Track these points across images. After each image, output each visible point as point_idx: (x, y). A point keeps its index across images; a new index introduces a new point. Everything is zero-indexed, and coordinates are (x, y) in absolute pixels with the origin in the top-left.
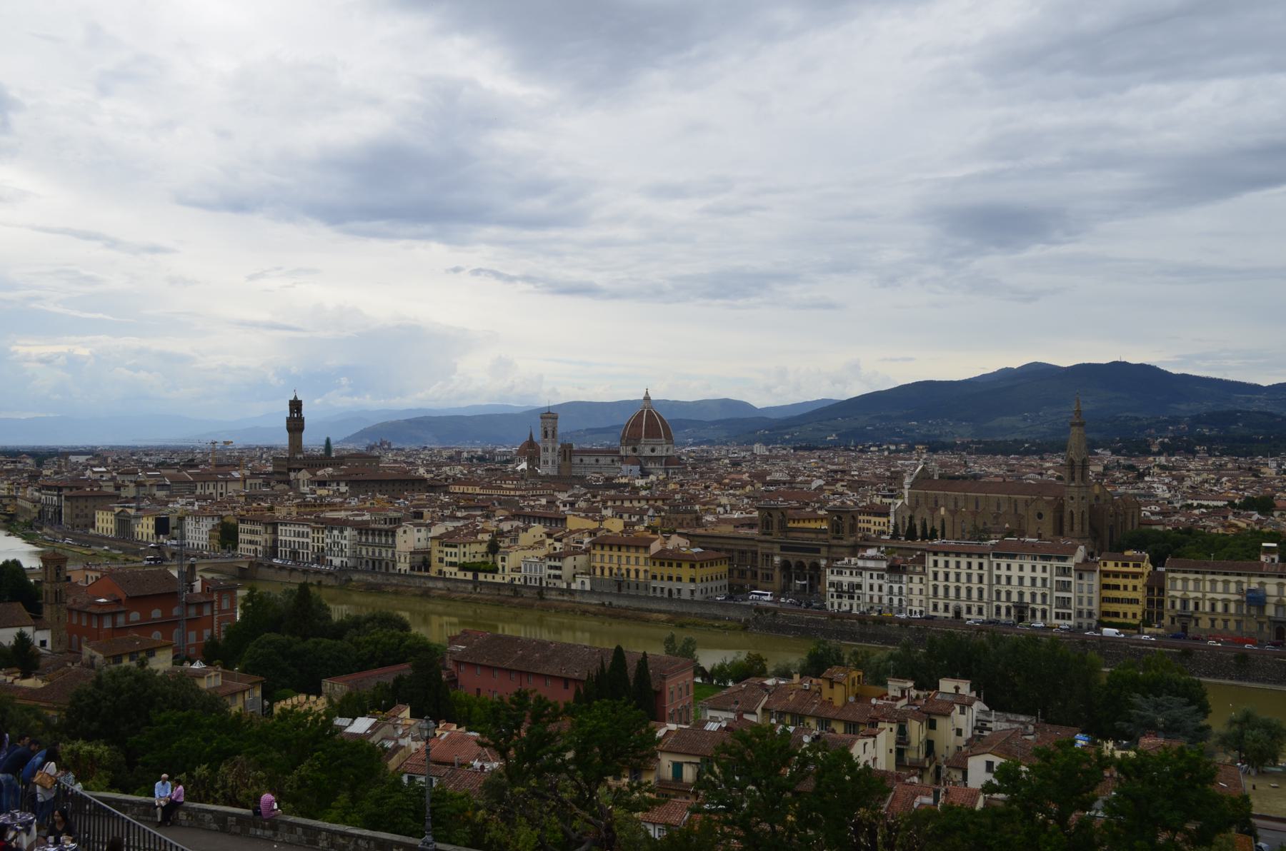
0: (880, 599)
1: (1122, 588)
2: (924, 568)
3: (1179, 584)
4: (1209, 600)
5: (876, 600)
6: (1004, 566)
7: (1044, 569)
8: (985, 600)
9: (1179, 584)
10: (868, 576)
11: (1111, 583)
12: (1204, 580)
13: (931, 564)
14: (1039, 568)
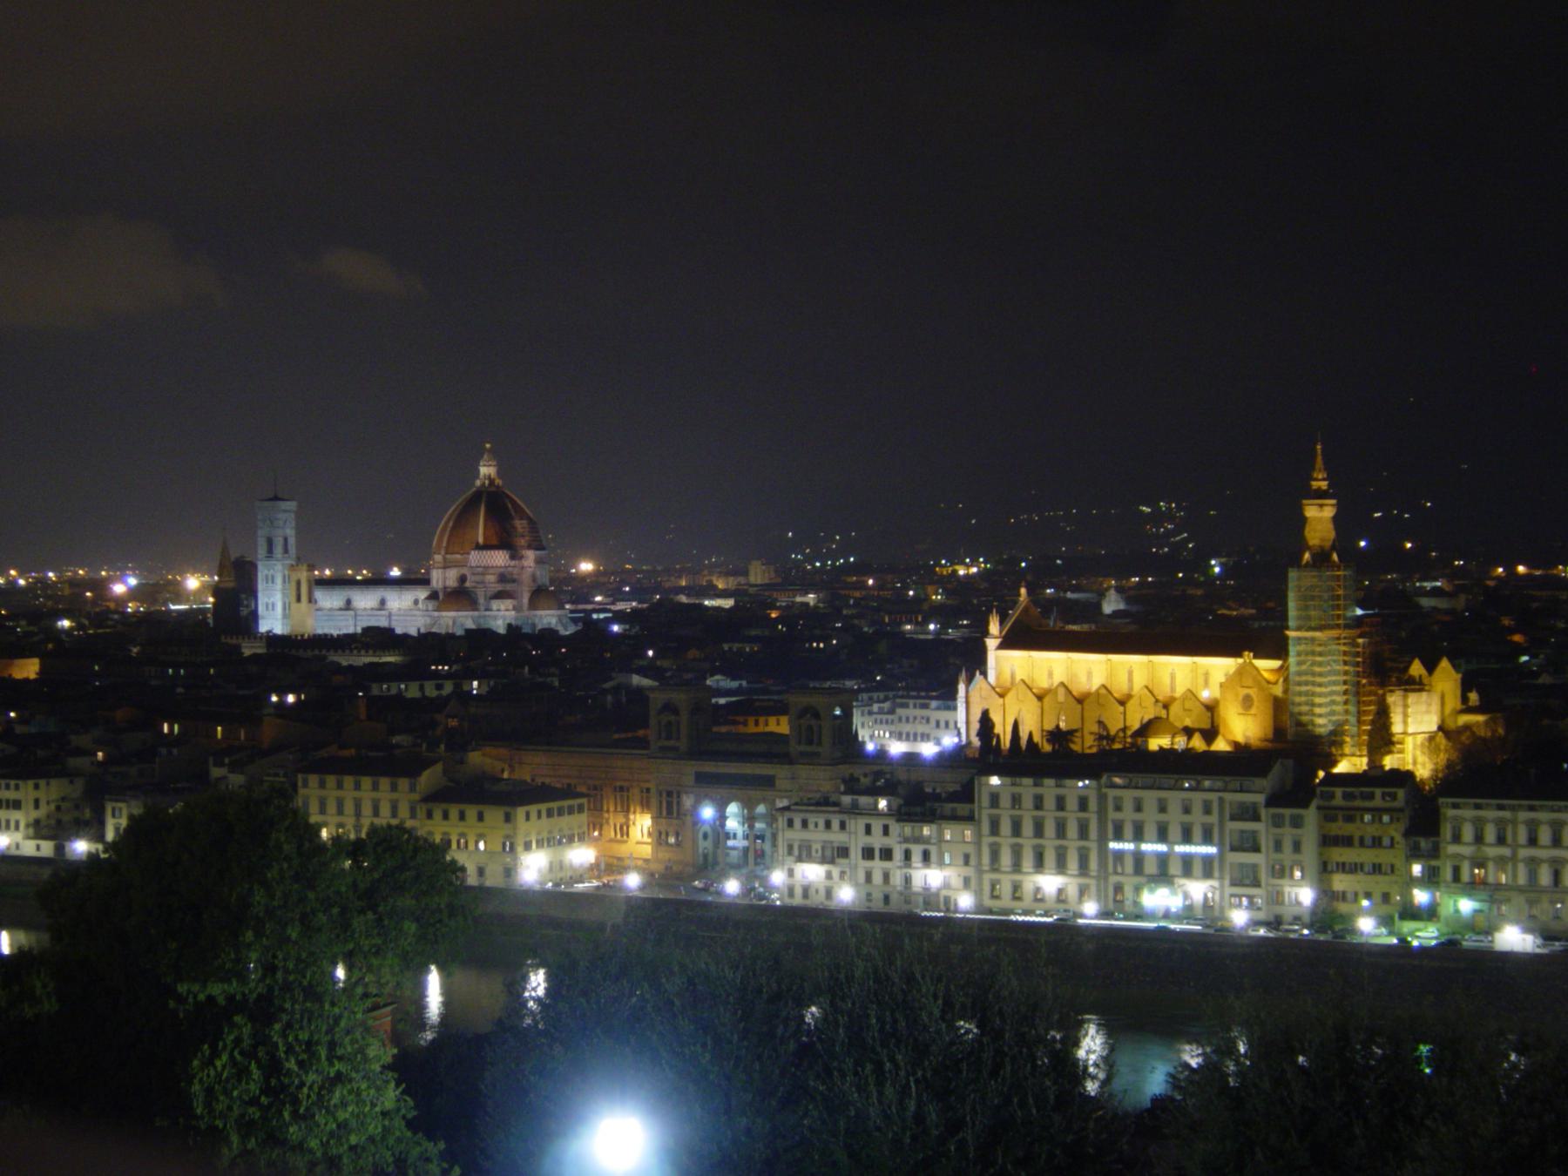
0: (886, 877)
1: (1356, 842)
2: (972, 811)
3: (1468, 833)
4: (1523, 860)
5: (877, 878)
6: (1128, 805)
7: (1207, 810)
8: (1093, 874)
9: (1468, 833)
10: (862, 829)
11: (1340, 833)
12: (1514, 822)
13: (985, 801)
14: (1197, 809)
